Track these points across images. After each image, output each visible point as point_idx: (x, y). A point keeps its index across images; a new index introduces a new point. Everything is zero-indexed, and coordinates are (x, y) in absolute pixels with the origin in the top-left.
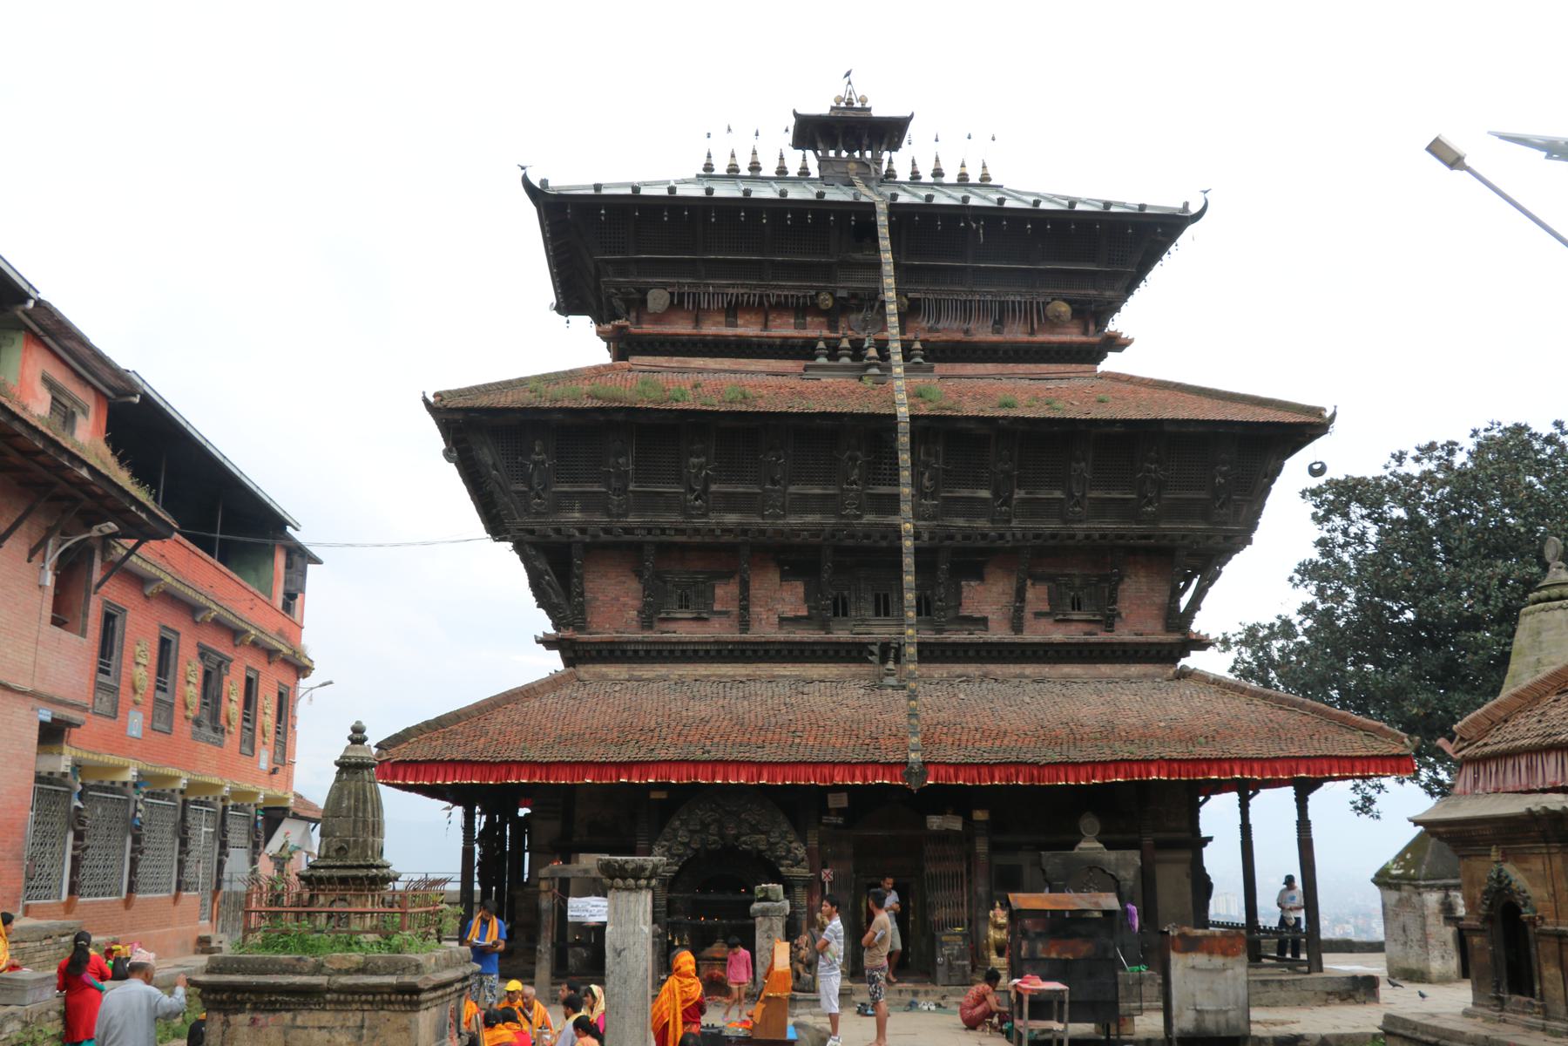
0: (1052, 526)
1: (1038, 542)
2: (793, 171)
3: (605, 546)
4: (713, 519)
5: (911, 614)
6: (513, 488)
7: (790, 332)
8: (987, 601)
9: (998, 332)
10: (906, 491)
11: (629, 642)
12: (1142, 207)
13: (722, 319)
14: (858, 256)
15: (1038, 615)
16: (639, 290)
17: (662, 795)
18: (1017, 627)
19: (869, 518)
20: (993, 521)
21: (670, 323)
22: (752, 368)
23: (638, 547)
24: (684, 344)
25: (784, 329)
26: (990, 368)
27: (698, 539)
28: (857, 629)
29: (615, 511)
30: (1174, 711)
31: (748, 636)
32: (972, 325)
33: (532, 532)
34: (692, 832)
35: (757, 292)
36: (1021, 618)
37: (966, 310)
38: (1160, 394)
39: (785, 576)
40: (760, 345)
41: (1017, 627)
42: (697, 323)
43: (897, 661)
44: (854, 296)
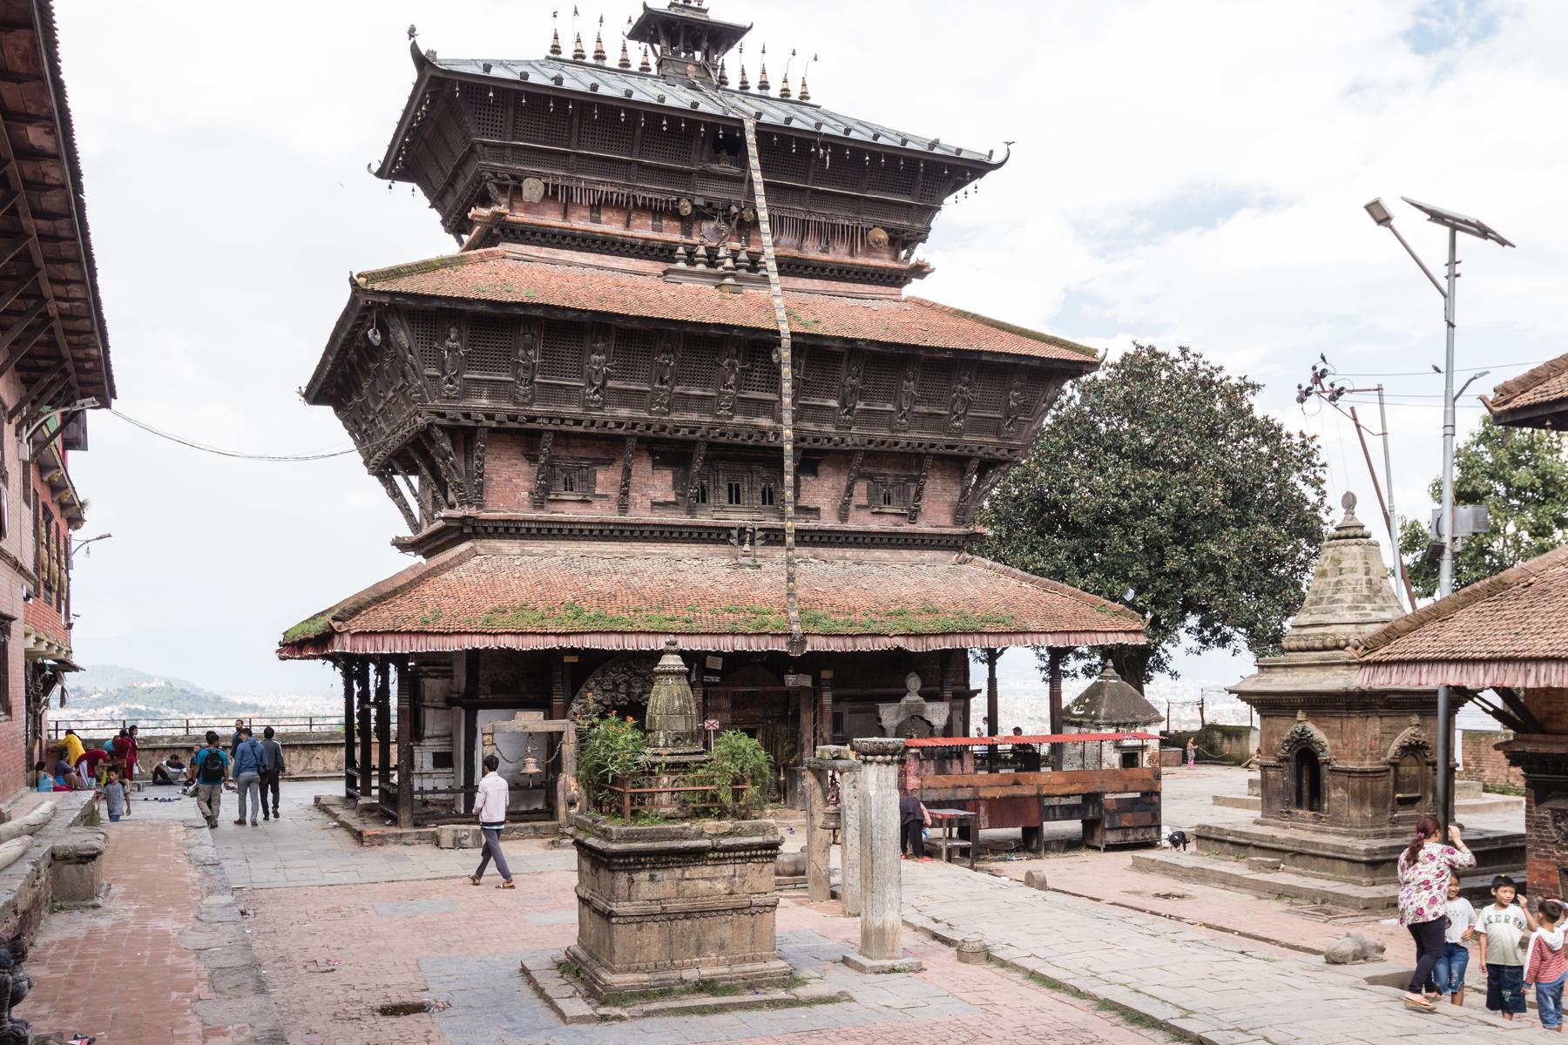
0: (882, 433)
1: (871, 447)
2: (635, 67)
3: (509, 431)
4: (608, 412)
5: (790, 509)
6: (427, 372)
7: (650, 234)
8: (823, 493)
9: (824, 251)
10: (787, 400)
11: (524, 521)
12: (959, 151)
13: (587, 214)
14: (715, 167)
15: (859, 507)
16: (514, 177)
17: (574, 659)
18: (843, 518)
19: (738, 419)
20: (838, 427)
21: (539, 213)
22: (614, 265)
23: (539, 433)
24: (554, 236)
25: (643, 230)
26: (816, 284)
27: (594, 430)
28: (716, 515)
29: (521, 400)
30: (971, 591)
31: (627, 518)
32: (808, 243)
33: (442, 415)
34: (605, 691)
35: (625, 192)
36: (847, 510)
37: (803, 229)
38: (965, 324)
39: (656, 465)
40: (623, 244)
41: (843, 518)
42: (565, 215)
43: (752, 543)
44: (709, 205)
